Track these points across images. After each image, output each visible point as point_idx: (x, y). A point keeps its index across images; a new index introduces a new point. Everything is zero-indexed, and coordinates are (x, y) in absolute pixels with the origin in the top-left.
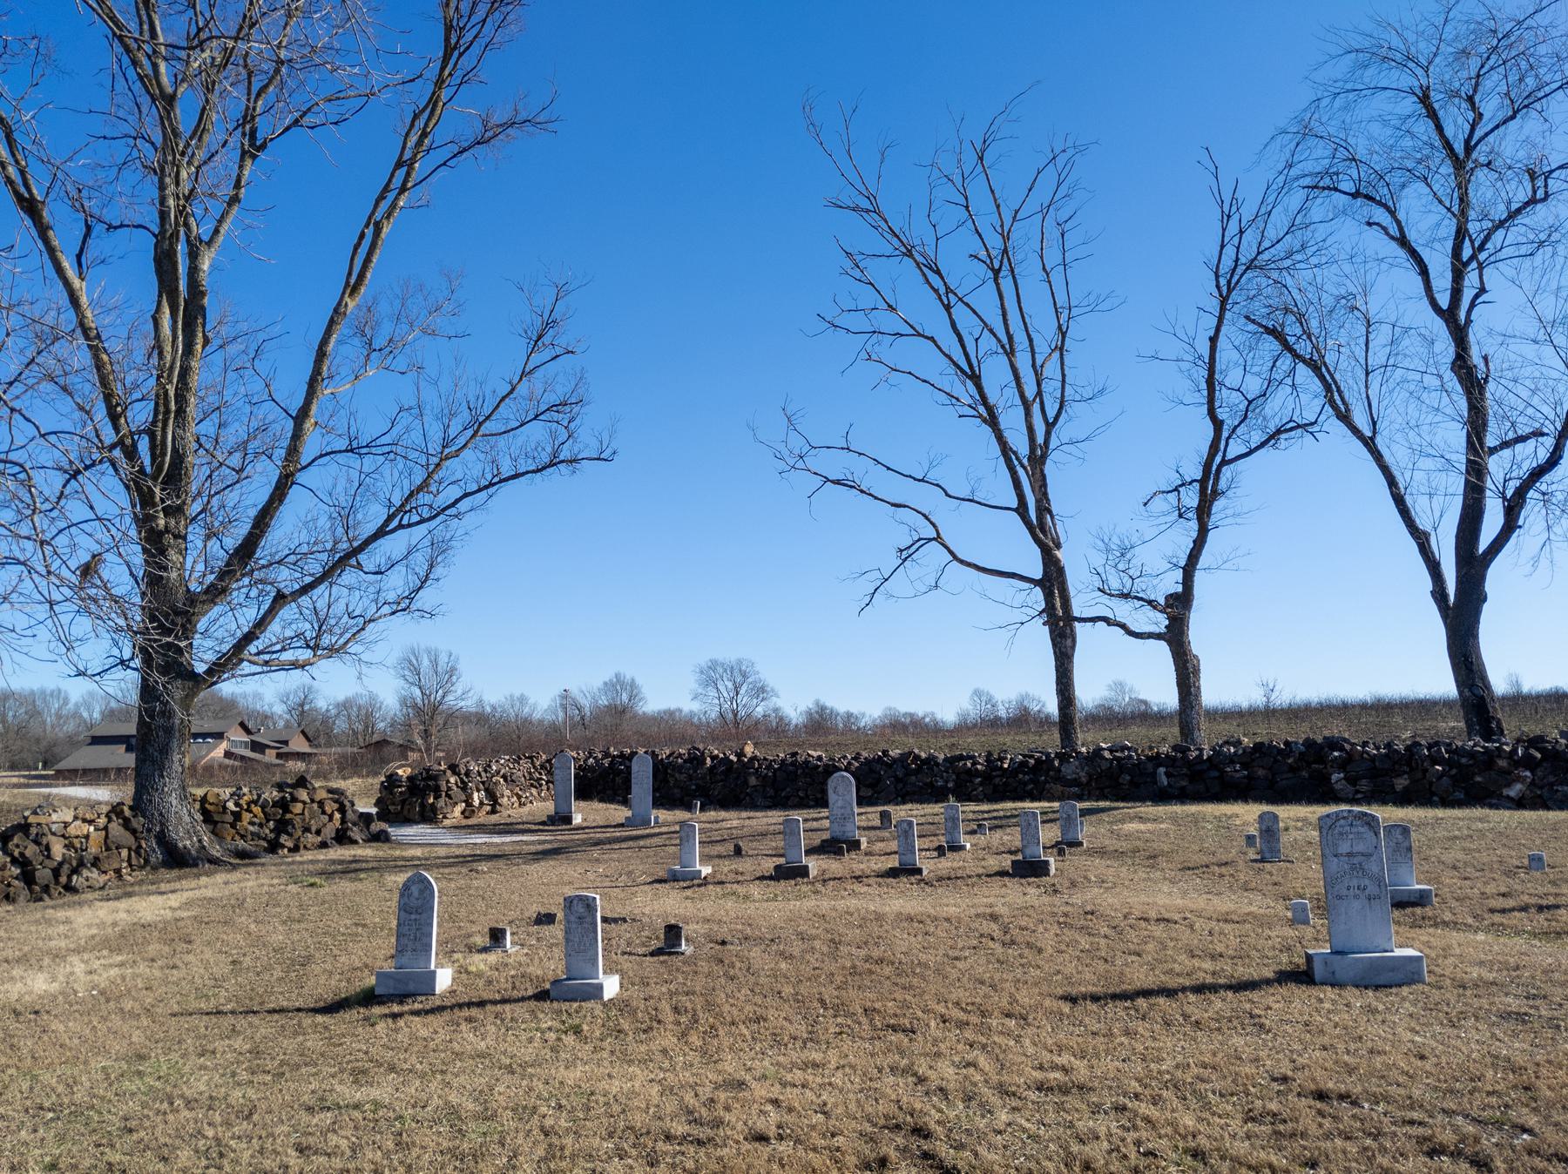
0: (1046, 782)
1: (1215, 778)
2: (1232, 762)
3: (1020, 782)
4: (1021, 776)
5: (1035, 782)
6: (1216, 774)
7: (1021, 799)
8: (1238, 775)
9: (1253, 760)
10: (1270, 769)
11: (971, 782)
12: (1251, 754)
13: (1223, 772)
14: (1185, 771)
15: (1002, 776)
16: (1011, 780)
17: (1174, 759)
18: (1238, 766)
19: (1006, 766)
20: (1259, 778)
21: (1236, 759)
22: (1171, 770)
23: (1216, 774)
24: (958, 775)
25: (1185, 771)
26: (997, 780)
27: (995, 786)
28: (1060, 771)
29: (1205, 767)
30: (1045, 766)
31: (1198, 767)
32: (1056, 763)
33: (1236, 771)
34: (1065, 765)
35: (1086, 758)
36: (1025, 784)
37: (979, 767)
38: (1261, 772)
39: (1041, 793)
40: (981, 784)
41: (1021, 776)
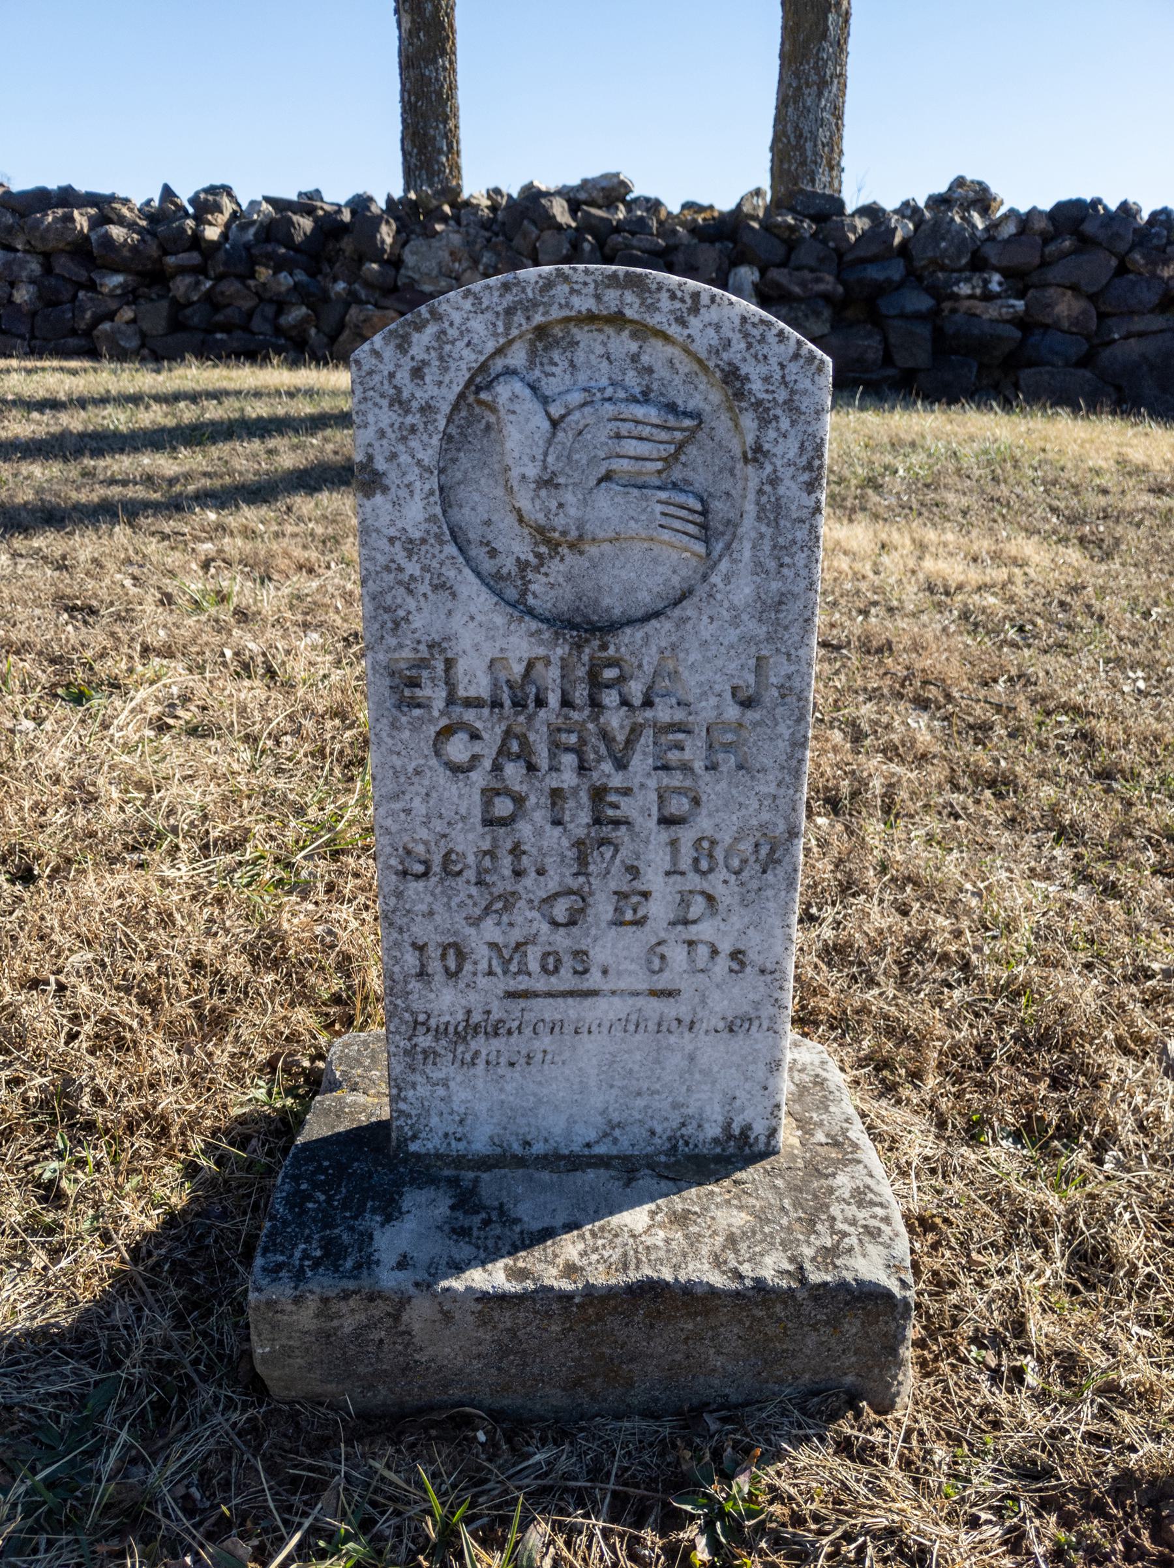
0: (352, 299)
1: (918, 316)
2: (978, 264)
3: (262, 295)
4: (264, 273)
5: (316, 300)
6: (923, 303)
7: (253, 355)
8: (991, 311)
9: (1044, 264)
10: (1092, 298)
11: (92, 286)
12: (1047, 239)
13: (941, 294)
14: (828, 283)
15: (200, 271)
16: (230, 287)
17: (790, 241)
18: (995, 282)
19: (212, 233)
20: (1056, 326)
21: (992, 253)
22: (775, 274)
23: (923, 303)
24: (47, 258)
25: (828, 283)
26: (181, 286)
27: (177, 306)
28: (396, 263)
29: (896, 271)
30: (347, 244)
31: (874, 273)
32: (387, 234)
33: (988, 297)
34: (416, 243)
35: (486, 225)
36: (281, 306)
37: (117, 232)
38: (1066, 307)
39: (333, 339)
40: (130, 296)
41: (264, 273)
